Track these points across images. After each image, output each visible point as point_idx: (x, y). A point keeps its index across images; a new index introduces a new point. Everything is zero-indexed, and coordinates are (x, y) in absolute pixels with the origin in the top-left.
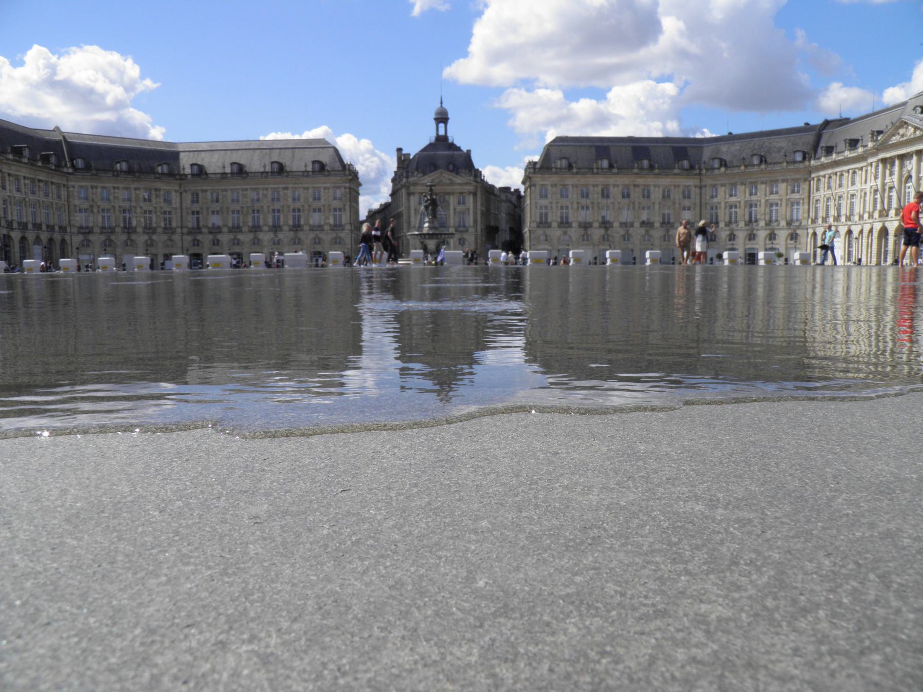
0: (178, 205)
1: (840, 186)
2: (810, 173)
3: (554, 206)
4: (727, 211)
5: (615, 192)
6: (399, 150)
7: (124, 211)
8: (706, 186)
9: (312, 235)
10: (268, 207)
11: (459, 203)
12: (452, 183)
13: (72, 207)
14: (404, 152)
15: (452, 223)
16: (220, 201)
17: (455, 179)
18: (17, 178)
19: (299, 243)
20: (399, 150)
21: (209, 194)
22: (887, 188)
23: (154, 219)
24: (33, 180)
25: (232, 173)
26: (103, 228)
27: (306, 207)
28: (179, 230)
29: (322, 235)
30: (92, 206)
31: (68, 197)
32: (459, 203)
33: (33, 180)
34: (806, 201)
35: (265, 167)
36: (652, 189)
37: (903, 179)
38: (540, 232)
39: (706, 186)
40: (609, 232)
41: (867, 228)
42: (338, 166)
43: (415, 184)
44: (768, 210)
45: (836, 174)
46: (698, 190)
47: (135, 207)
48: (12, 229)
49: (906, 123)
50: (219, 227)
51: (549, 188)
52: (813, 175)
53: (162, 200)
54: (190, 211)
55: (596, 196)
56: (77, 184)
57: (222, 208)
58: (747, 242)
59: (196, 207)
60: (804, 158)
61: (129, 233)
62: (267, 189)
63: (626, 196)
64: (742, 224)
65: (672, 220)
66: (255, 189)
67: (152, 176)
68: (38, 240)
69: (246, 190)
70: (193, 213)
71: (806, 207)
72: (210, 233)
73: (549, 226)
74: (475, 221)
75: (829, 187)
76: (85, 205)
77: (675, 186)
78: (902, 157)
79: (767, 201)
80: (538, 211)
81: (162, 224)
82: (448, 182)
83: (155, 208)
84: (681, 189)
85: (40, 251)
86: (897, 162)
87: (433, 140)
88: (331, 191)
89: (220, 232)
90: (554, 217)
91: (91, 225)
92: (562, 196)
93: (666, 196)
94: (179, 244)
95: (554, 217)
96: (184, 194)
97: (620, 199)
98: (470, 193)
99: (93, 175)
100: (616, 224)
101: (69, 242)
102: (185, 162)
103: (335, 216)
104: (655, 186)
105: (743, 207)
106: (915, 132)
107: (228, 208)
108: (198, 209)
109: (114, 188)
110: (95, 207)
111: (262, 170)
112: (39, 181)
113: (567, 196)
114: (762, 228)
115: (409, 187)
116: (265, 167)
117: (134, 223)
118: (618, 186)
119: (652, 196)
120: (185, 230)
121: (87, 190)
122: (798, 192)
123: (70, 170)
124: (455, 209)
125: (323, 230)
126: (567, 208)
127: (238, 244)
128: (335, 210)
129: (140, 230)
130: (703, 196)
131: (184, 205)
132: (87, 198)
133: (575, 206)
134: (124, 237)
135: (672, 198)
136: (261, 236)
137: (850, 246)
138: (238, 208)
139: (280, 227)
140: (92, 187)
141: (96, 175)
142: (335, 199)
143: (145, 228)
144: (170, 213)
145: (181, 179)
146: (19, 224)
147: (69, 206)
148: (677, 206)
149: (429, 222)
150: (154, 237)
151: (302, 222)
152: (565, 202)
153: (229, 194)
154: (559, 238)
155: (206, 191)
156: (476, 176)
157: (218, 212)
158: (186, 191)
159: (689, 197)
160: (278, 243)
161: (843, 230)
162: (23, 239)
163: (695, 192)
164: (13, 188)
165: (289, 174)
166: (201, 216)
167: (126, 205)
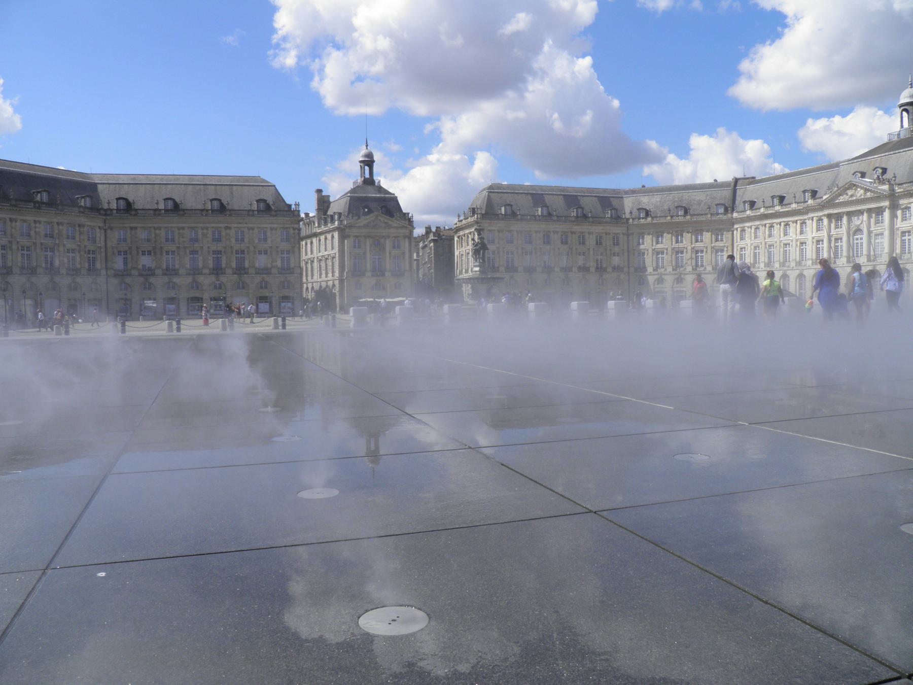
0: (103, 244)
1: (770, 236)
2: (733, 224)
6: (319, 191)
8: (633, 234)
9: (258, 279)
11: (394, 247)
14: (324, 194)
17: (390, 223)
19: (243, 288)
20: (319, 191)
22: (833, 239)
23: (78, 259)
25: (118, 210)
27: (252, 248)
30: (10, 242)
32: (394, 247)
36: (587, 236)
37: (851, 233)
39: (633, 234)
44: (694, 256)
45: (765, 225)
46: (626, 238)
49: (855, 185)
50: (150, 269)
52: (736, 226)
54: (116, 251)
57: (154, 248)
58: (675, 285)
61: (217, 274)
62: (207, 228)
63: (599, 243)
64: (670, 269)
65: (604, 265)
66: (193, 228)
67: (76, 209)
69: (183, 228)
70: (119, 253)
72: (141, 275)
78: (850, 214)
79: (693, 248)
83: (79, 246)
84: (611, 236)
86: (845, 219)
89: (153, 275)
96: (109, 232)
98: (405, 237)
99: (11, 205)
103: (282, 259)
104: (589, 233)
105: (670, 253)
106: (865, 194)
107: (277, 247)
109: (35, 222)
111: (248, 208)
114: (690, 273)
116: (157, 203)
118: (557, 232)
119: (587, 243)
120: (111, 272)
121: (5, 223)
122: (722, 240)
125: (270, 273)
127: (173, 288)
129: (63, 271)
131: (109, 244)
135: (604, 244)
136: (200, 279)
138: (174, 248)
139: (244, 269)
140: (11, 220)
141: (15, 206)
145: (106, 215)
148: (608, 252)
149: (479, 266)
151: (247, 265)
153: (163, 233)
157: (149, 253)
158: (111, 228)
160: (220, 288)
165: (234, 212)
166: (129, 256)
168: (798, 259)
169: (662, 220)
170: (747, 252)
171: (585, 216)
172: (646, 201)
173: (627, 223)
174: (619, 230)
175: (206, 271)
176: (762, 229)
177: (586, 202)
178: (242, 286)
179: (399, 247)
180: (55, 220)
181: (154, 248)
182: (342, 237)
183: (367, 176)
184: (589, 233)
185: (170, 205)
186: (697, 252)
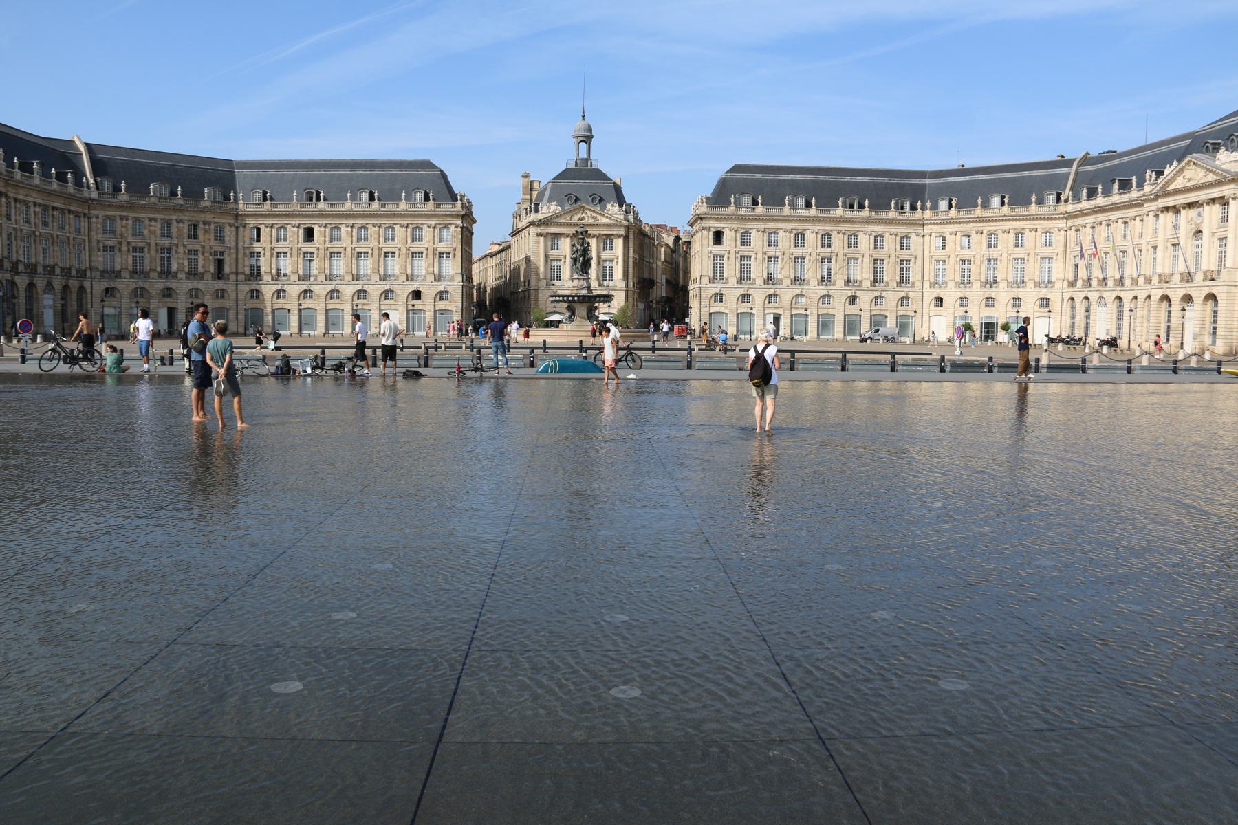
0: (233, 244)
3: (732, 255)
4: (958, 267)
6: (526, 176)
7: (162, 250)
10: (353, 249)
13: (94, 244)
18: (26, 203)
24: (45, 208)
28: (233, 277)
30: (120, 243)
31: (90, 230)
33: (45, 208)
41: (1142, 295)
48: (18, 273)
53: (212, 237)
56: (102, 213)
68: (49, 287)
71: (1062, 265)
82: (591, 221)
83: (203, 247)
85: (51, 302)
91: (118, 267)
96: (241, 229)
105: (978, 262)
109: (150, 220)
112: (54, 208)
117: (175, 267)
123: (94, 195)
124: (599, 257)
131: (241, 244)
132: (113, 232)
133: (760, 256)
137: (1120, 318)
144: (222, 253)
146: (26, 266)
147: (90, 242)
152: (745, 250)
161: (1110, 296)
162: (31, 285)
164: (21, 218)
167: (165, 242)
178: (387, 294)
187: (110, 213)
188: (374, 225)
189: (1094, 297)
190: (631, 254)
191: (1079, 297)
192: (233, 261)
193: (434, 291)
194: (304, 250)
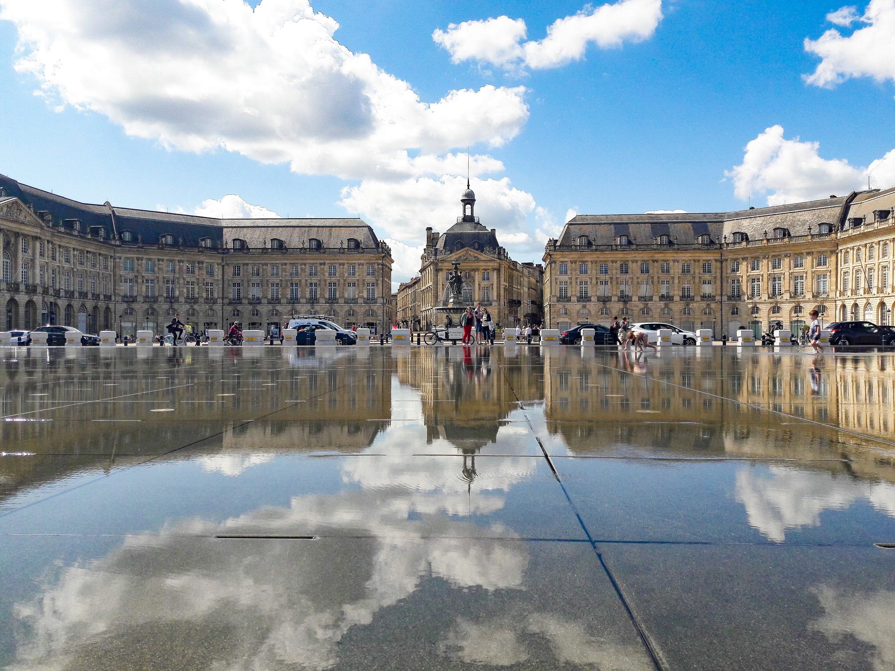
0: (220, 277)
5: (634, 268)
8: (727, 260)
9: (346, 307)
11: (484, 279)
12: (477, 260)
13: (117, 278)
15: (477, 298)
16: (261, 274)
17: (479, 257)
21: (250, 267)
23: (197, 290)
26: (147, 297)
27: (342, 281)
29: (356, 308)
31: (115, 267)
32: (484, 279)
34: (833, 273)
35: (303, 243)
38: (560, 306)
39: (727, 260)
40: (628, 306)
42: (372, 244)
43: (443, 261)
46: (719, 264)
47: (178, 278)
50: (258, 299)
51: (569, 264)
53: (204, 272)
55: (614, 271)
56: (124, 256)
57: (262, 281)
58: (772, 315)
59: (237, 279)
60: (830, 231)
61: (171, 302)
62: (305, 265)
63: (645, 271)
69: (286, 264)
70: (234, 285)
71: (834, 279)
72: (250, 303)
73: (569, 300)
74: (499, 295)
75: (858, 259)
76: (131, 275)
77: (695, 261)
79: (791, 274)
80: (558, 287)
81: (204, 295)
83: (198, 279)
84: (701, 264)
87: (460, 220)
88: (365, 267)
89: (260, 303)
90: (574, 291)
91: (135, 294)
92: (581, 272)
93: (685, 271)
94: (220, 314)
95: (574, 291)
97: (639, 274)
98: (494, 270)
99: (139, 247)
100: (635, 298)
101: (113, 310)
102: (228, 237)
103: (368, 290)
104: (674, 261)
105: (765, 279)
108: (239, 282)
109: (159, 260)
110: (140, 277)
111: (301, 246)
113: (586, 272)
114: (787, 301)
115: (437, 264)
116: (303, 243)
117: (177, 293)
118: (637, 262)
119: (672, 271)
121: (133, 261)
125: (356, 303)
126: (586, 283)
128: (368, 284)
129: (182, 299)
130: (724, 270)
133: (594, 281)
134: (166, 306)
135: (692, 272)
138: (278, 281)
140: (138, 259)
141: (142, 248)
142: (368, 274)
143: (187, 298)
148: (697, 280)
150: (196, 307)
154: (578, 312)
155: (247, 264)
156: (499, 253)
158: (228, 264)
159: (709, 271)
161: (875, 302)
163: (715, 266)
166: (241, 288)
167: (170, 276)
168: (880, 286)
169: (758, 245)
170: (850, 277)
171: (671, 243)
172: (747, 226)
173: (721, 248)
174: (711, 256)
175: (304, 301)
176: (863, 249)
177: (676, 231)
179: (488, 279)
180: (177, 259)
181: (262, 281)
182: (437, 271)
183: (468, 213)
184: (674, 261)
185: (276, 245)
186: (796, 278)
187: (128, 256)
188: (321, 264)
189: (861, 303)
190: (502, 282)
191: (849, 304)
192: (221, 290)
193: (363, 310)
194: (271, 281)
